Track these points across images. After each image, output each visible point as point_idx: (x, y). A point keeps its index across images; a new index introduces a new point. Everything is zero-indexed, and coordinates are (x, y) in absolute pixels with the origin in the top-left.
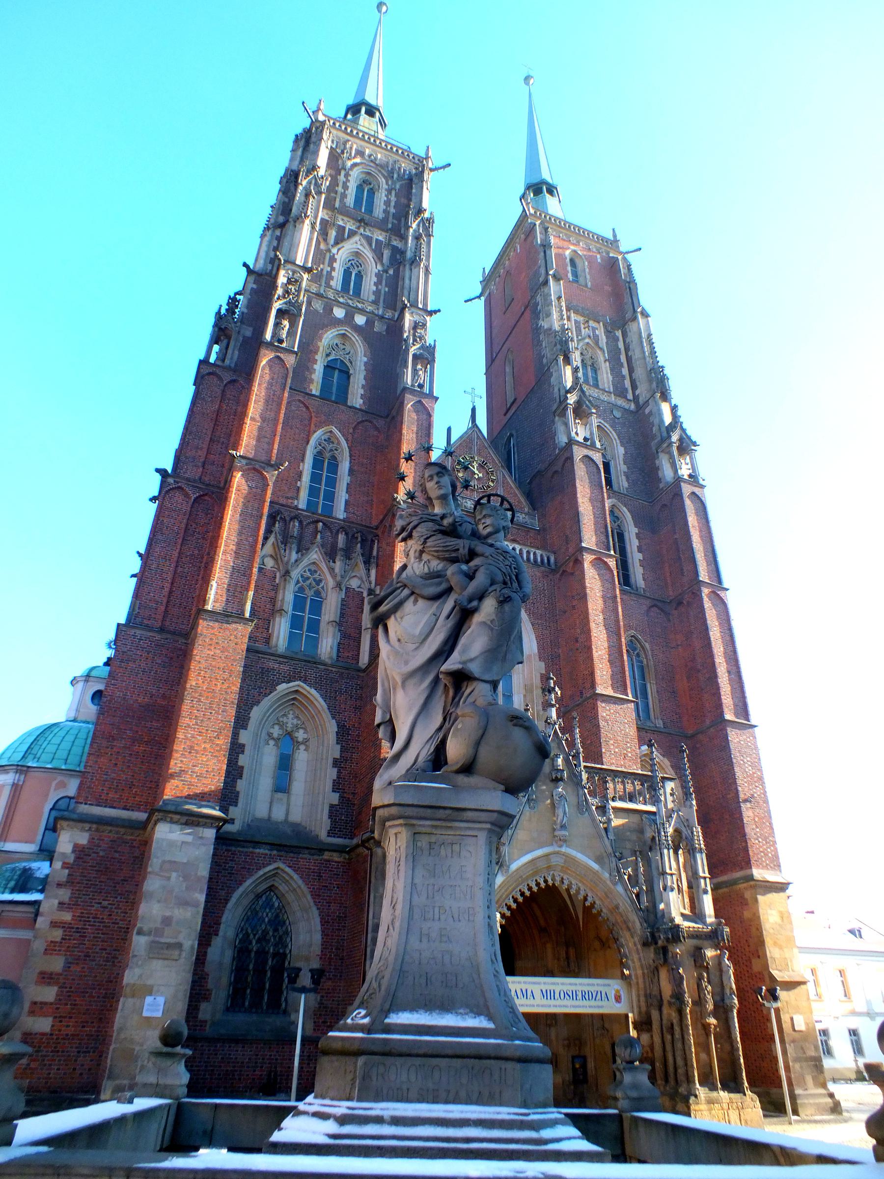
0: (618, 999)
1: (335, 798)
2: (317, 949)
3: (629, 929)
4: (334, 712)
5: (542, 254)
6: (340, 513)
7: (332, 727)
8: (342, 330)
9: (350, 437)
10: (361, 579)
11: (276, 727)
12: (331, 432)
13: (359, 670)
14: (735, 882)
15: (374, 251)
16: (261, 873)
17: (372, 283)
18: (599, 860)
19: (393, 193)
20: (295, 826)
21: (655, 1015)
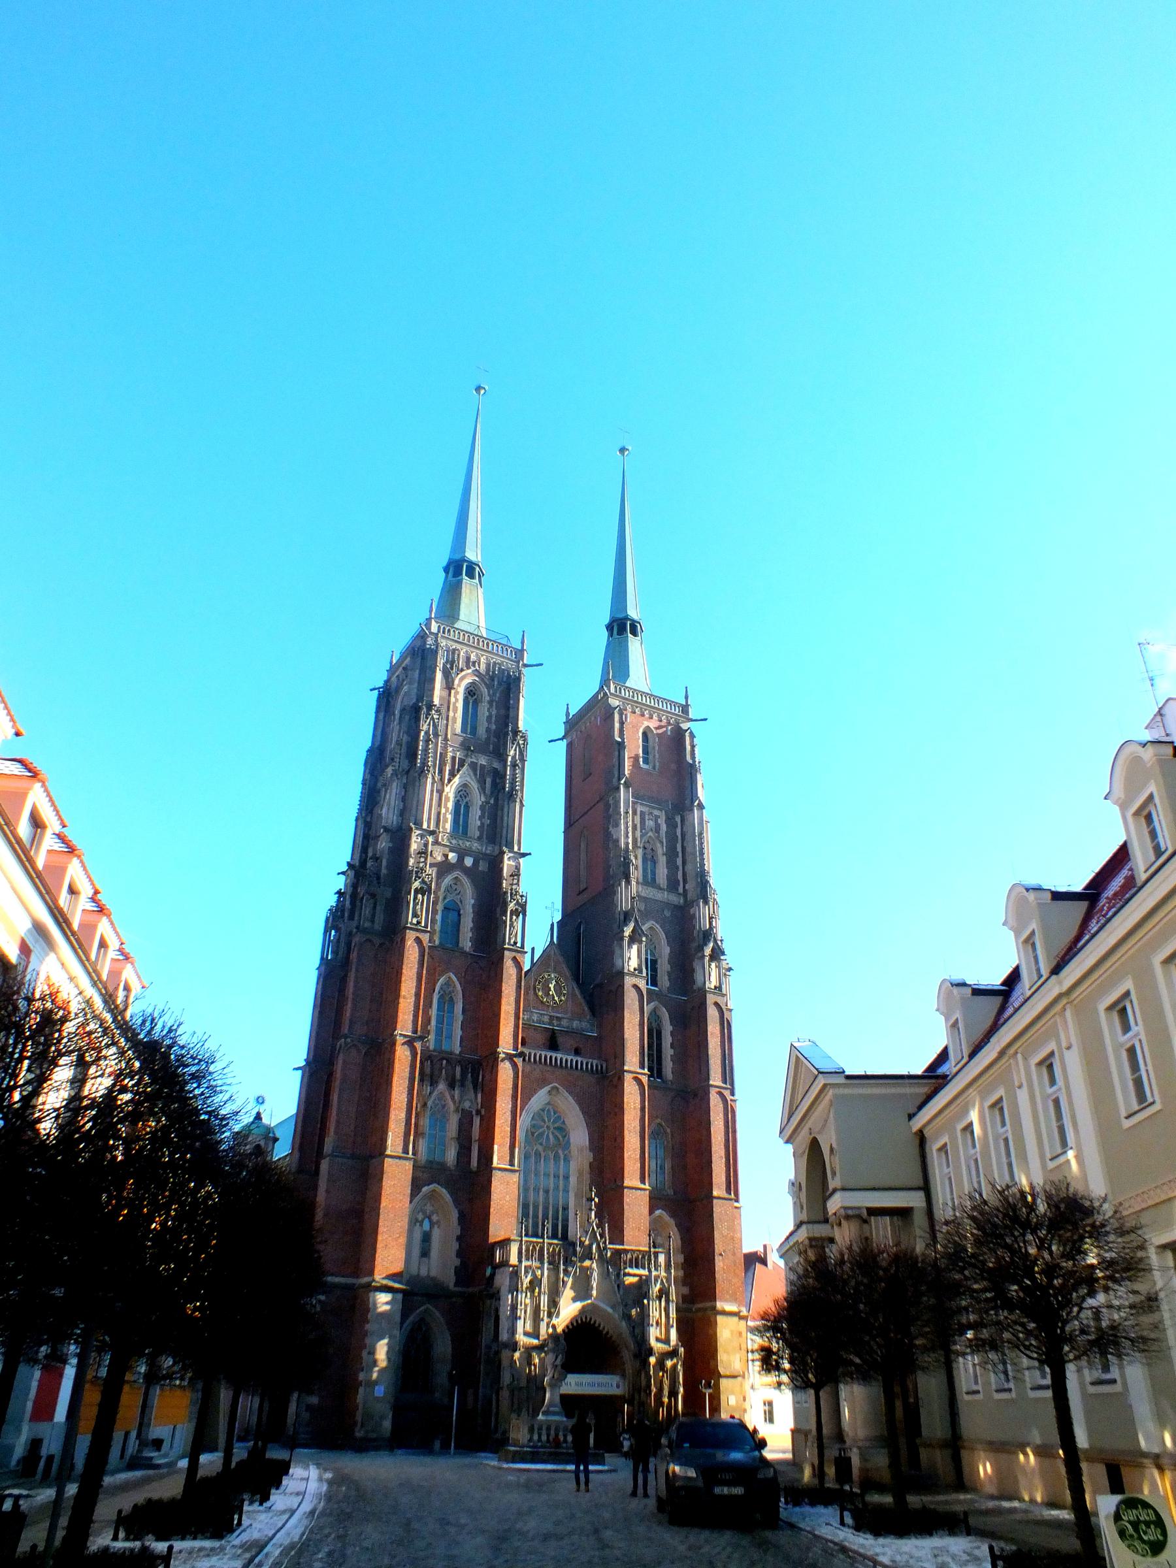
0: (618, 1386)
1: (457, 1262)
2: (450, 1357)
3: (627, 1348)
4: (457, 1202)
5: (617, 753)
6: (457, 1050)
7: (455, 1214)
8: (456, 874)
9: (463, 979)
10: (471, 1101)
11: (421, 1213)
12: (449, 977)
13: (471, 1172)
14: (705, 1310)
15: (478, 781)
16: (418, 1311)
17: (477, 818)
18: (613, 1307)
19: (494, 704)
20: (433, 1279)
21: (637, 1397)
